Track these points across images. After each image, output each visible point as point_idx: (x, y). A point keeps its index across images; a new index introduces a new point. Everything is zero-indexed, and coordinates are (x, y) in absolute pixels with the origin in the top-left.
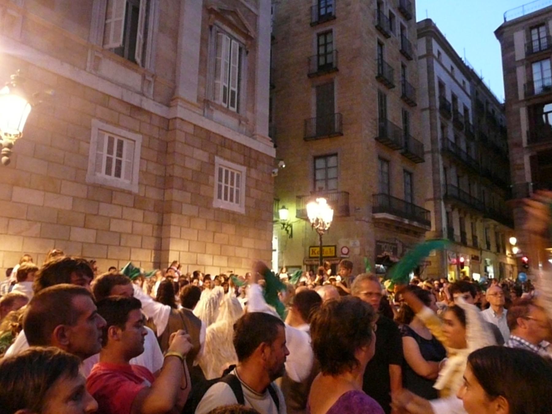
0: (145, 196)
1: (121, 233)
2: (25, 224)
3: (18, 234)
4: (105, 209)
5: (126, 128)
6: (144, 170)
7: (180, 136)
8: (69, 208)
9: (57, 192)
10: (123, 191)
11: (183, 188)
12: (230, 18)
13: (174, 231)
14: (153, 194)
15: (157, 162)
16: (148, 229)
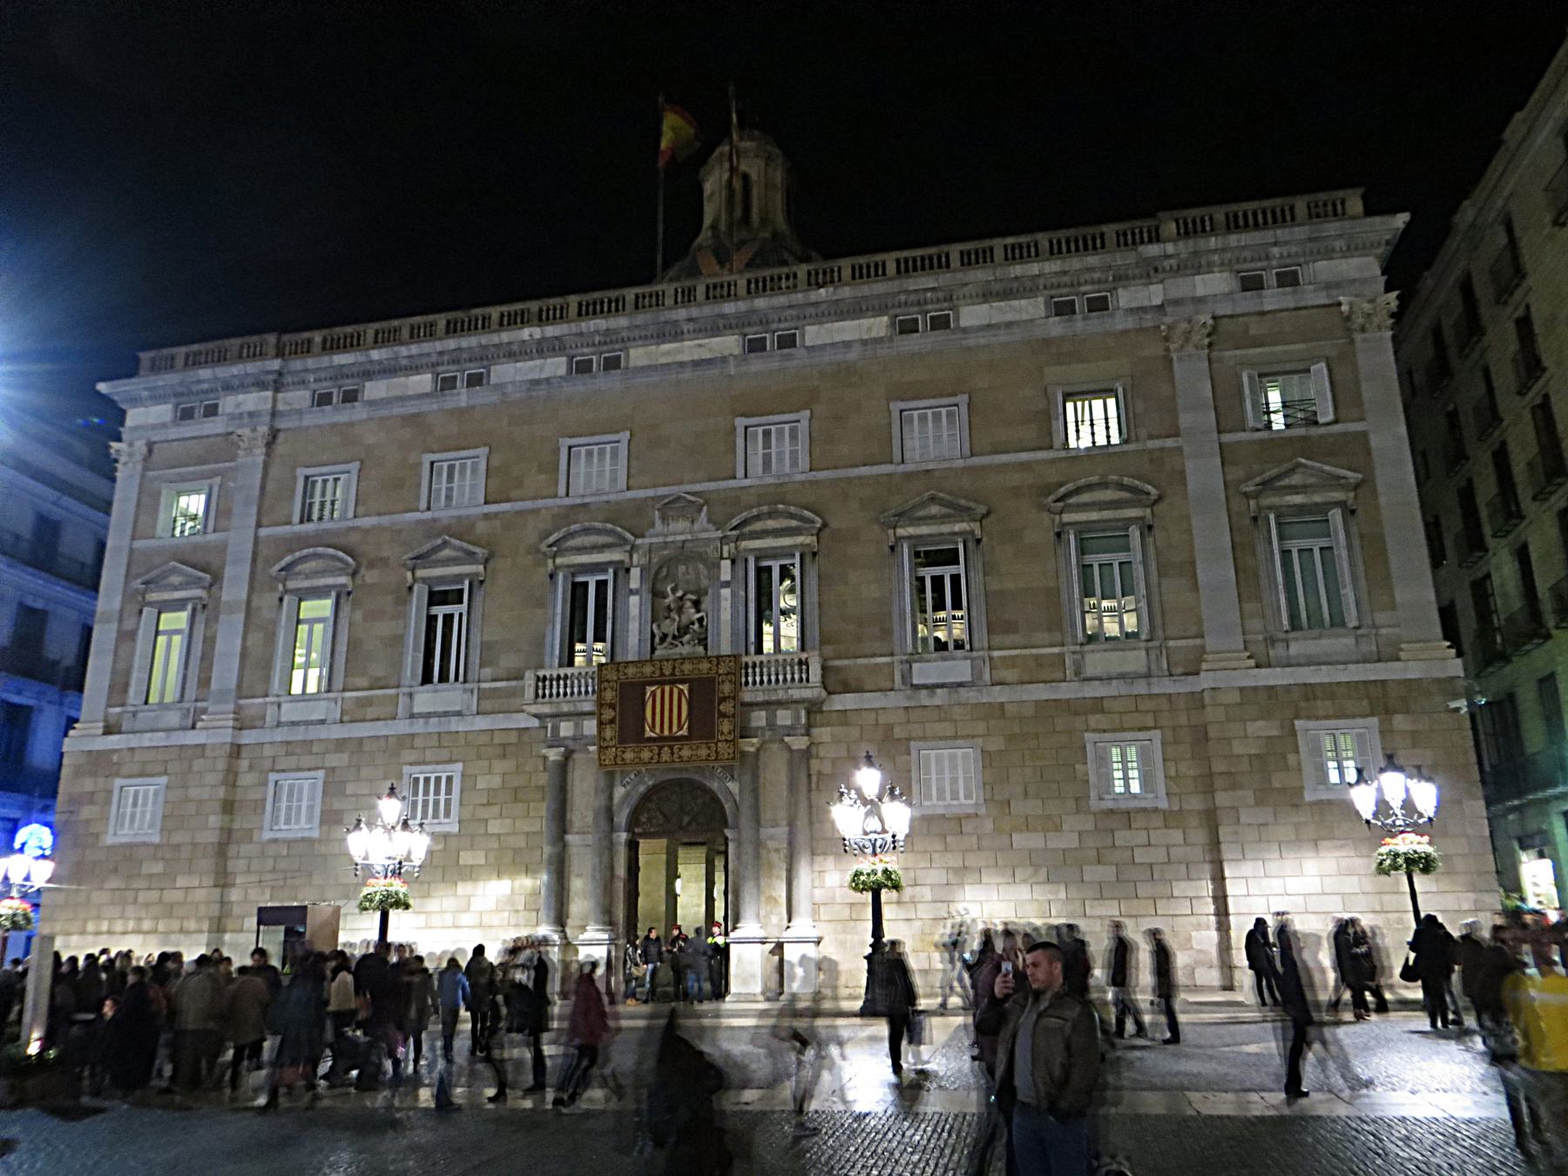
0: (1181, 810)
1: (1151, 865)
2: (1030, 870)
3: (1024, 881)
4: (1122, 837)
5: (1132, 729)
6: (1173, 773)
7: (1213, 714)
8: (1075, 844)
9: (1058, 829)
10: (1144, 810)
11: (1234, 786)
12: (1296, 479)
13: (1227, 852)
14: (1195, 803)
15: (1193, 758)
16: (1197, 853)
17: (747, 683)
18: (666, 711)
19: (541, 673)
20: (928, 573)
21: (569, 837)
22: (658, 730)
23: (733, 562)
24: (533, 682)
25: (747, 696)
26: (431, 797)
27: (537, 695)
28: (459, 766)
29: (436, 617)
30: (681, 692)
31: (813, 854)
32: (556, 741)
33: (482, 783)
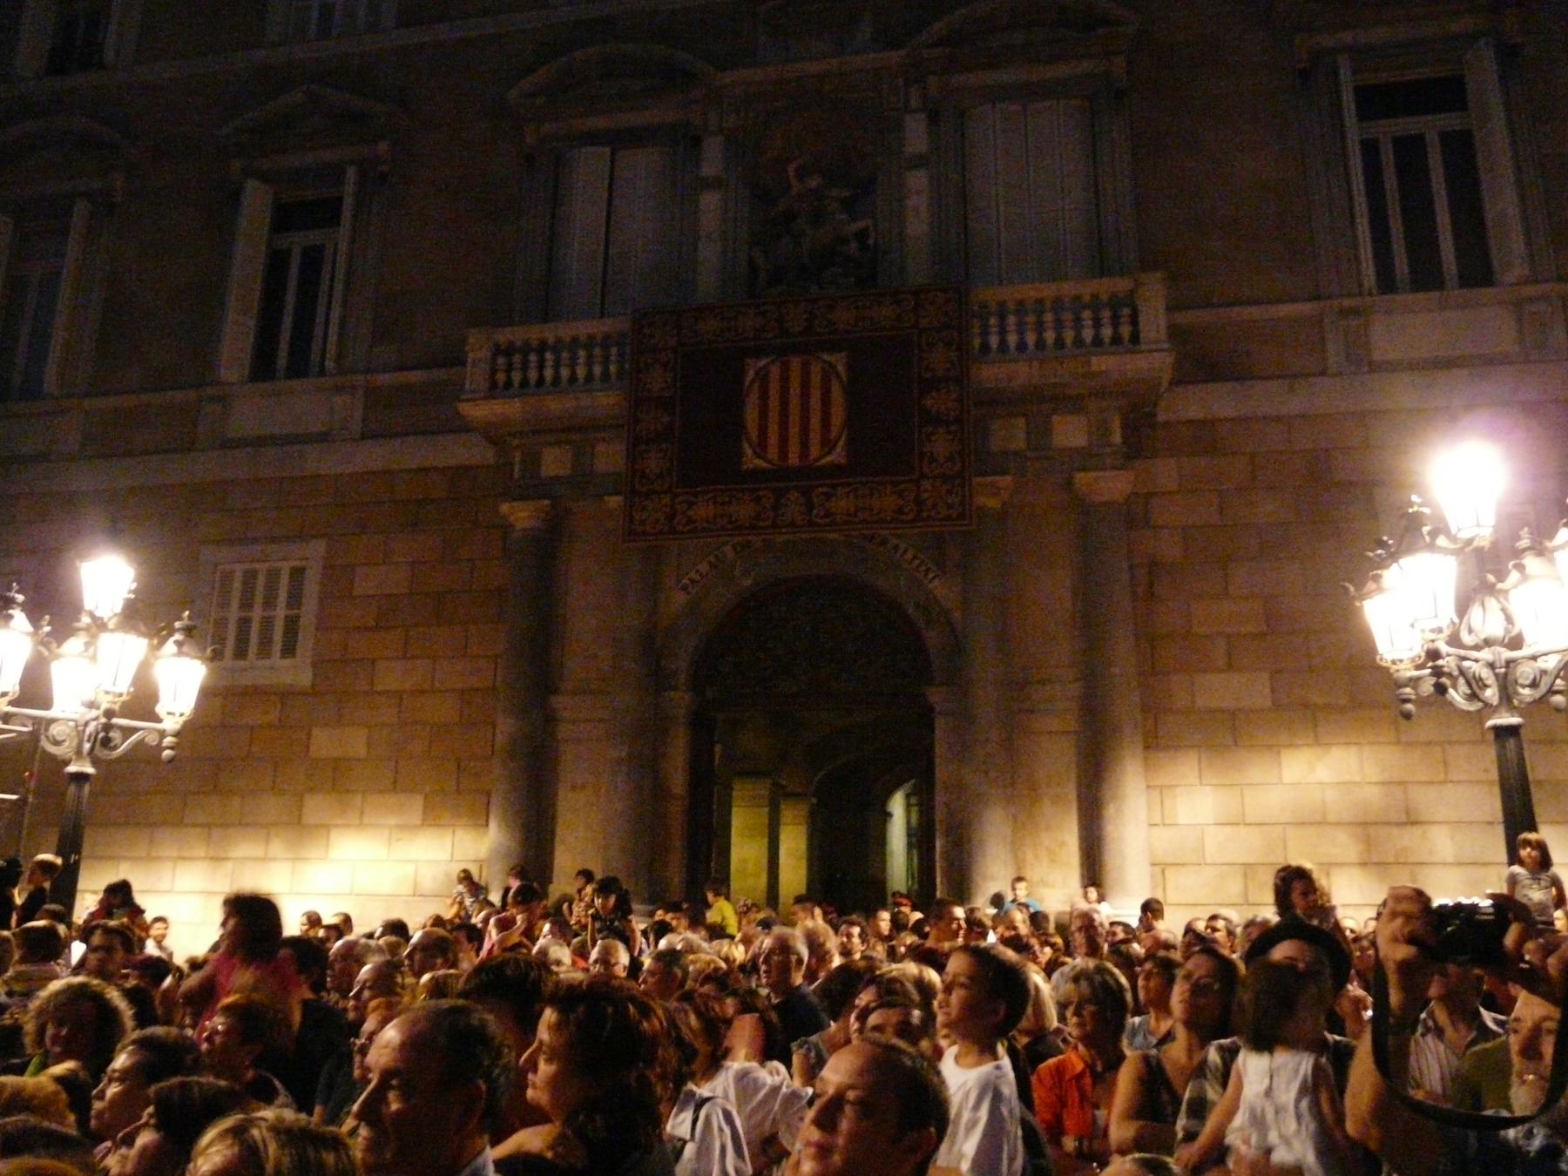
17: (985, 347)
18: (796, 411)
19: (504, 336)
20: (1388, 129)
21: (558, 701)
22: (773, 453)
23: (934, 118)
24: (485, 353)
25: (989, 374)
26: (257, 614)
27: (493, 385)
28: (318, 548)
29: (288, 252)
30: (828, 373)
31: (1147, 747)
32: (533, 487)
33: (367, 583)
